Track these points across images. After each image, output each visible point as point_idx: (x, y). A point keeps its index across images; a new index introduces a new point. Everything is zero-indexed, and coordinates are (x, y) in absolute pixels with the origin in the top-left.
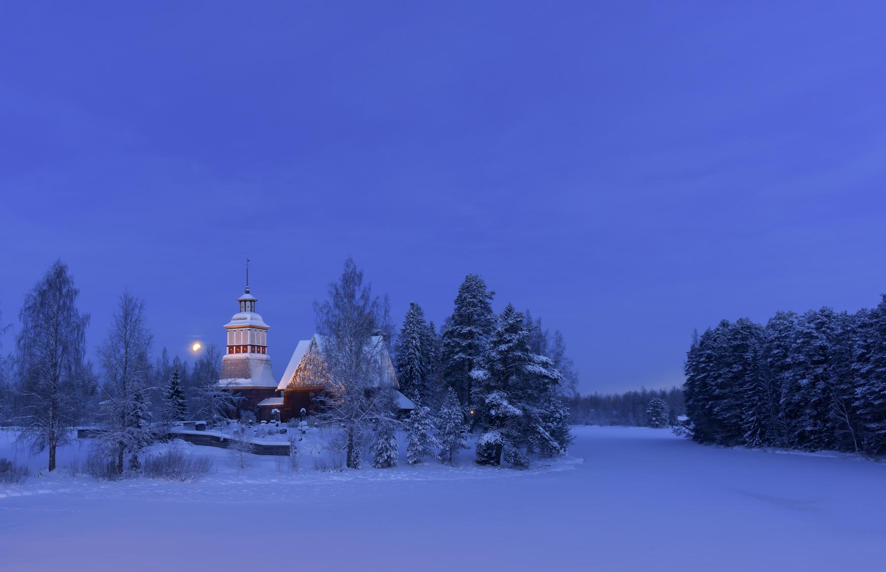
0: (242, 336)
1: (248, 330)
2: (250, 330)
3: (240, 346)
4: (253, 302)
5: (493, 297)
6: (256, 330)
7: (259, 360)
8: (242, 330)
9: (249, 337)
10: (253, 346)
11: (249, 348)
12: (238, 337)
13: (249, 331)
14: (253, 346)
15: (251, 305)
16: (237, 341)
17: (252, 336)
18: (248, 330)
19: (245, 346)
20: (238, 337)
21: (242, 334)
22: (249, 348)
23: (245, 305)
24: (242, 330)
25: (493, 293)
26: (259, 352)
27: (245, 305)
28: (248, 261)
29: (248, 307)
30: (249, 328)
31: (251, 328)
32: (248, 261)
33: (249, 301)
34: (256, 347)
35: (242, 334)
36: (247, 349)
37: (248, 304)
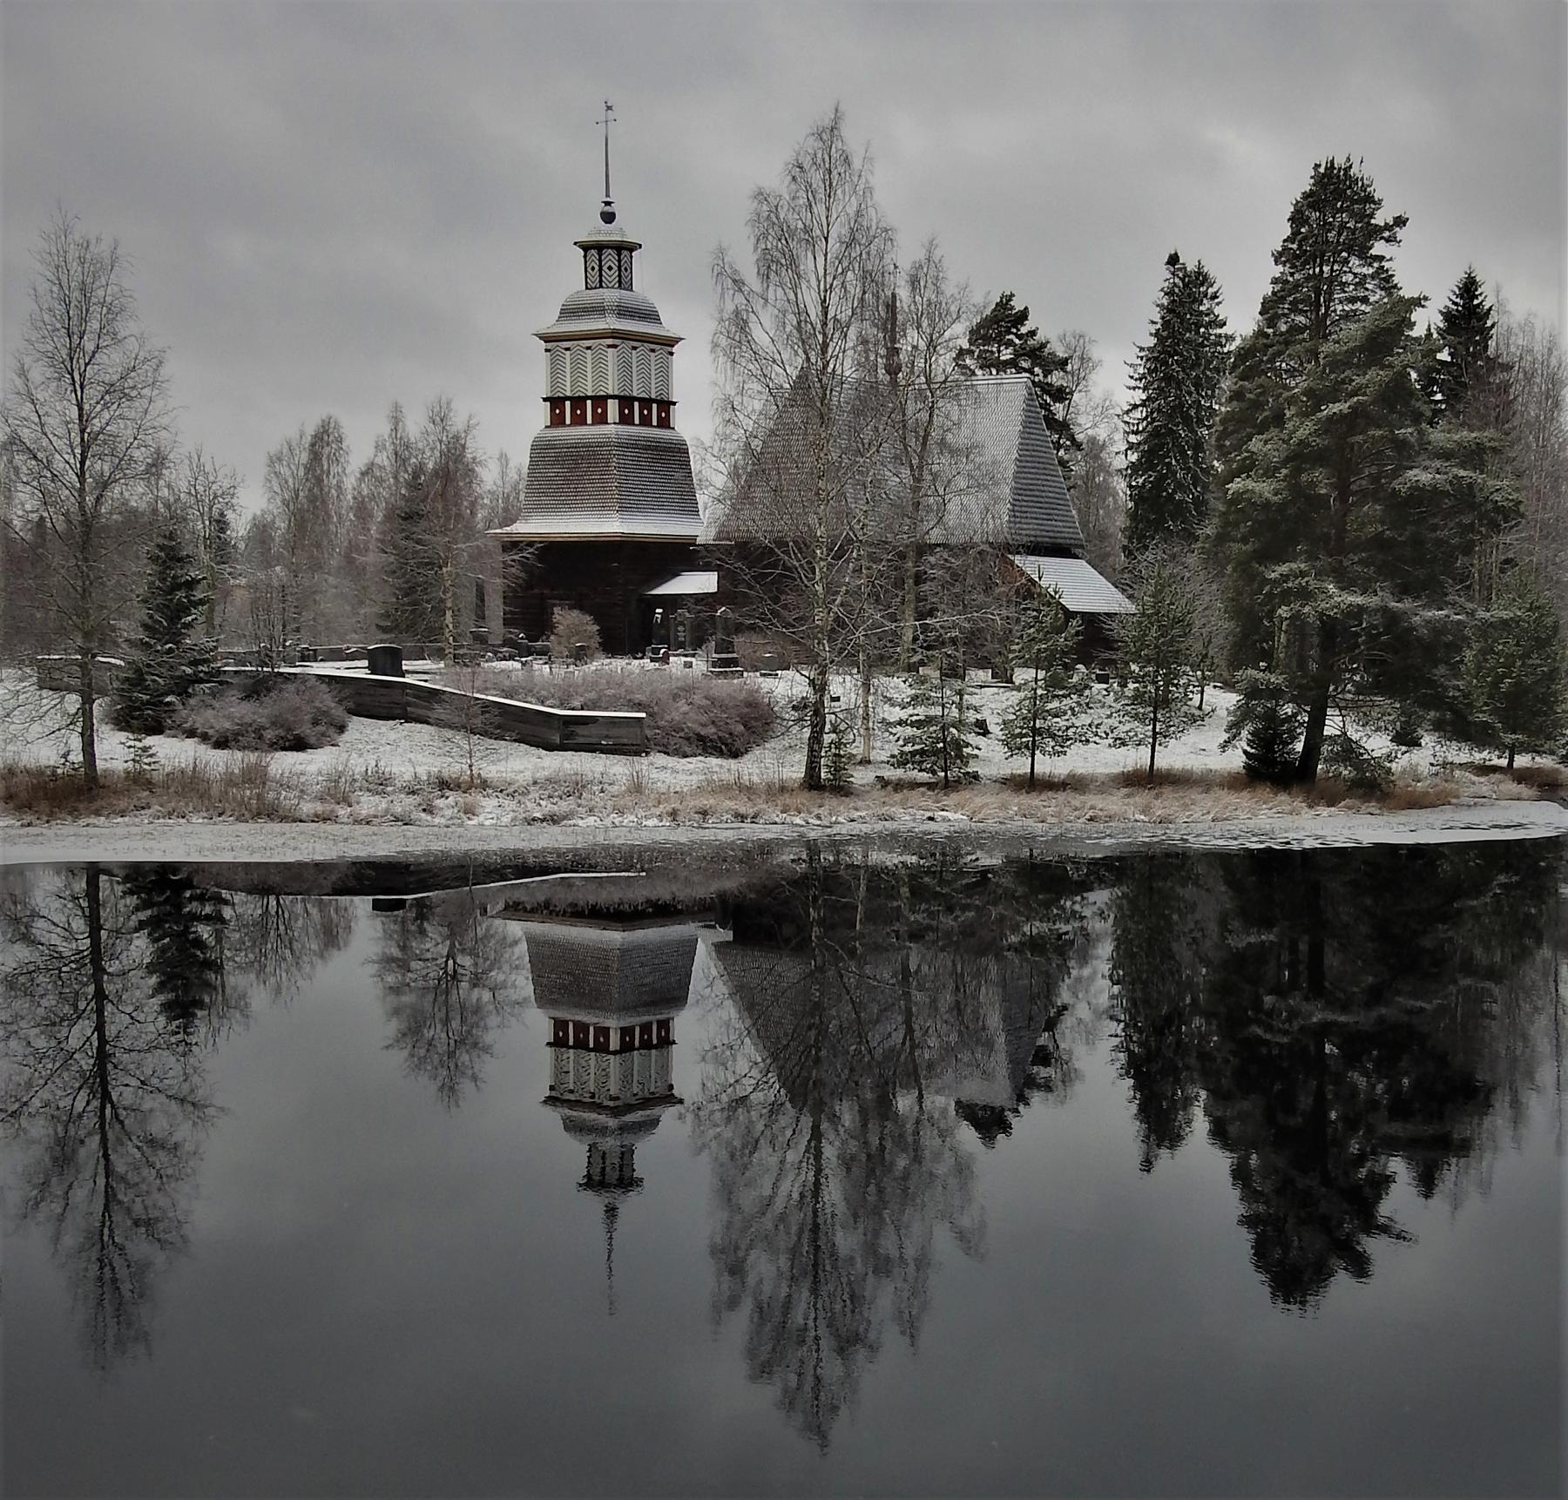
0: (589, 366)
1: (609, 346)
2: (615, 346)
4: (625, 253)
5: (1400, 233)
6: (635, 348)
7: (635, 446)
8: (589, 348)
9: (610, 364)
10: (625, 401)
12: (577, 367)
13: (610, 350)
14: (625, 401)
15: (619, 261)
17: (625, 368)
18: (609, 346)
19: (600, 401)
20: (577, 367)
21: (589, 361)
22: (613, 407)
23: (600, 261)
24: (589, 348)
25: (1400, 222)
26: (646, 421)
27: (600, 261)
28: (609, 108)
29: (610, 268)
30: (610, 342)
31: (617, 342)
33: (612, 248)
34: (636, 404)
35: (589, 361)
37: (610, 257)
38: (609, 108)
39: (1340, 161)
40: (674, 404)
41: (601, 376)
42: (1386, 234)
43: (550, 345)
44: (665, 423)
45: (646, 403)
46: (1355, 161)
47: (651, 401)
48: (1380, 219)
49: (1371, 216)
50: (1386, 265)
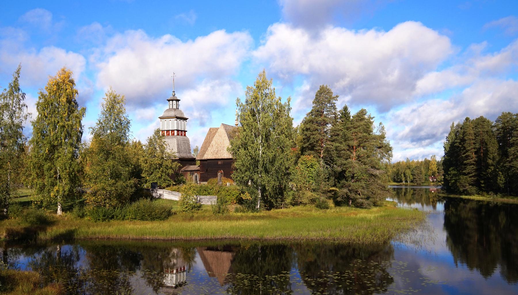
3: (169, 130)
11: (176, 132)
14: (178, 131)
16: (167, 127)
17: (178, 124)
19: (173, 131)
25: (337, 97)
26: (182, 135)
32: (174, 74)
36: (174, 133)
38: (174, 74)
39: (325, 86)
40: (187, 131)
41: (173, 126)
42: (335, 99)
43: (161, 120)
44: (185, 135)
45: (182, 131)
46: (328, 85)
47: (179, 130)
48: (334, 95)
49: (331, 96)
50: (335, 104)
